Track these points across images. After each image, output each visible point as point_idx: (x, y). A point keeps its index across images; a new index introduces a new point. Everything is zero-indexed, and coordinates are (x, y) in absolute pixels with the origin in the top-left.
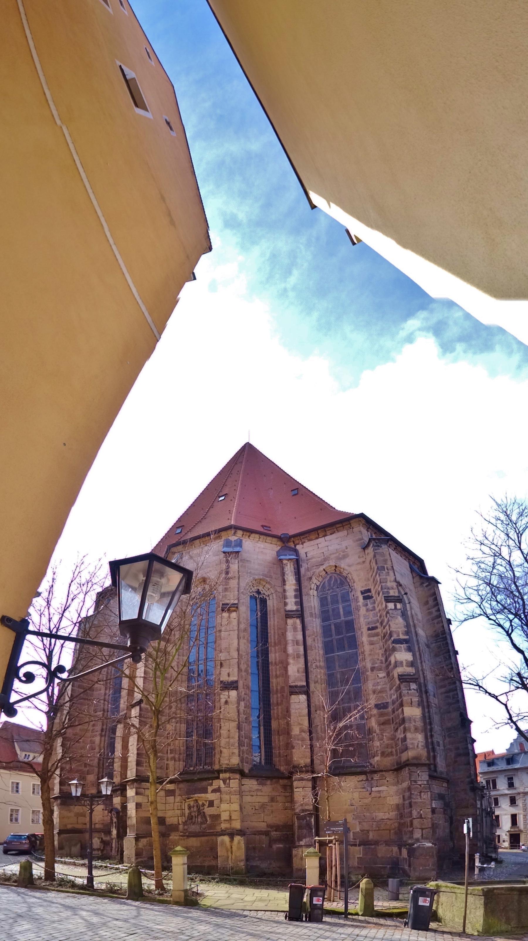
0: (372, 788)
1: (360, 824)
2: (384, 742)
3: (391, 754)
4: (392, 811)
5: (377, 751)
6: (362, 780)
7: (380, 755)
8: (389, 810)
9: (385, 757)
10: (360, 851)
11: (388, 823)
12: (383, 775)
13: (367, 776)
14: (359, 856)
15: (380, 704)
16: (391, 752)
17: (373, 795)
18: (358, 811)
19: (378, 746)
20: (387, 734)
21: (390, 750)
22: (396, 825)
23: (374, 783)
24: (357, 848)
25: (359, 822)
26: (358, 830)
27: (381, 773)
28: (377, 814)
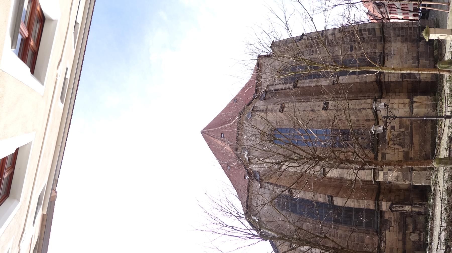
0: (392, 54)
1: (409, 60)
2: (369, 48)
3: (375, 45)
4: (404, 45)
5: (373, 51)
6: (387, 58)
7: (375, 50)
8: (403, 47)
9: (377, 47)
10: (422, 60)
11: (409, 47)
12: (386, 49)
13: (386, 56)
14: (424, 60)
15: (350, 49)
16: (374, 44)
17: (395, 53)
18: (403, 61)
19: (371, 50)
20: (365, 46)
21: (373, 45)
22: (410, 43)
23: (389, 53)
24: (420, 61)
25: (408, 60)
26: (411, 61)
27: (385, 49)
28: (405, 52)
